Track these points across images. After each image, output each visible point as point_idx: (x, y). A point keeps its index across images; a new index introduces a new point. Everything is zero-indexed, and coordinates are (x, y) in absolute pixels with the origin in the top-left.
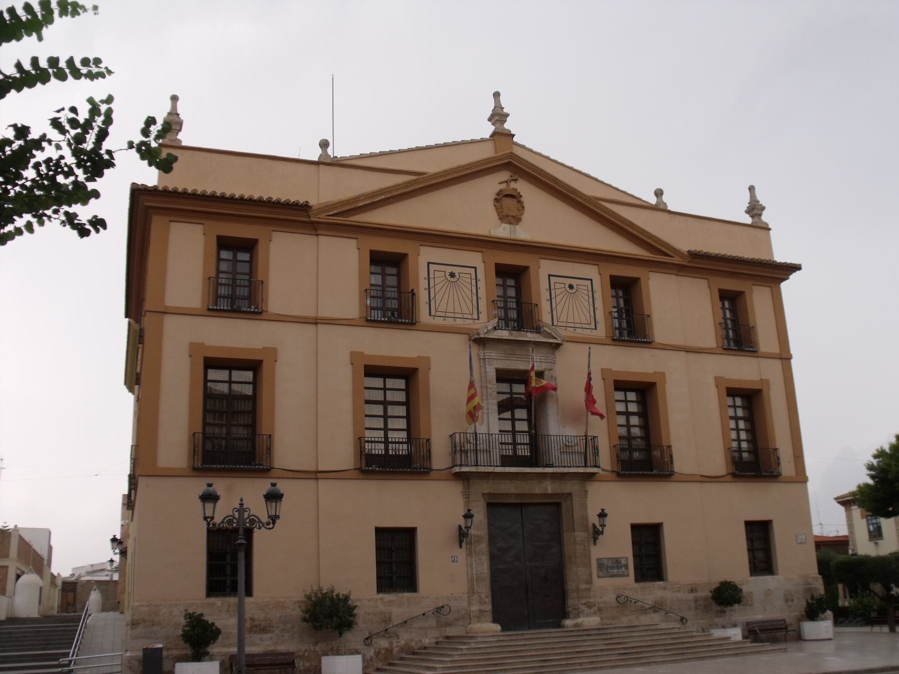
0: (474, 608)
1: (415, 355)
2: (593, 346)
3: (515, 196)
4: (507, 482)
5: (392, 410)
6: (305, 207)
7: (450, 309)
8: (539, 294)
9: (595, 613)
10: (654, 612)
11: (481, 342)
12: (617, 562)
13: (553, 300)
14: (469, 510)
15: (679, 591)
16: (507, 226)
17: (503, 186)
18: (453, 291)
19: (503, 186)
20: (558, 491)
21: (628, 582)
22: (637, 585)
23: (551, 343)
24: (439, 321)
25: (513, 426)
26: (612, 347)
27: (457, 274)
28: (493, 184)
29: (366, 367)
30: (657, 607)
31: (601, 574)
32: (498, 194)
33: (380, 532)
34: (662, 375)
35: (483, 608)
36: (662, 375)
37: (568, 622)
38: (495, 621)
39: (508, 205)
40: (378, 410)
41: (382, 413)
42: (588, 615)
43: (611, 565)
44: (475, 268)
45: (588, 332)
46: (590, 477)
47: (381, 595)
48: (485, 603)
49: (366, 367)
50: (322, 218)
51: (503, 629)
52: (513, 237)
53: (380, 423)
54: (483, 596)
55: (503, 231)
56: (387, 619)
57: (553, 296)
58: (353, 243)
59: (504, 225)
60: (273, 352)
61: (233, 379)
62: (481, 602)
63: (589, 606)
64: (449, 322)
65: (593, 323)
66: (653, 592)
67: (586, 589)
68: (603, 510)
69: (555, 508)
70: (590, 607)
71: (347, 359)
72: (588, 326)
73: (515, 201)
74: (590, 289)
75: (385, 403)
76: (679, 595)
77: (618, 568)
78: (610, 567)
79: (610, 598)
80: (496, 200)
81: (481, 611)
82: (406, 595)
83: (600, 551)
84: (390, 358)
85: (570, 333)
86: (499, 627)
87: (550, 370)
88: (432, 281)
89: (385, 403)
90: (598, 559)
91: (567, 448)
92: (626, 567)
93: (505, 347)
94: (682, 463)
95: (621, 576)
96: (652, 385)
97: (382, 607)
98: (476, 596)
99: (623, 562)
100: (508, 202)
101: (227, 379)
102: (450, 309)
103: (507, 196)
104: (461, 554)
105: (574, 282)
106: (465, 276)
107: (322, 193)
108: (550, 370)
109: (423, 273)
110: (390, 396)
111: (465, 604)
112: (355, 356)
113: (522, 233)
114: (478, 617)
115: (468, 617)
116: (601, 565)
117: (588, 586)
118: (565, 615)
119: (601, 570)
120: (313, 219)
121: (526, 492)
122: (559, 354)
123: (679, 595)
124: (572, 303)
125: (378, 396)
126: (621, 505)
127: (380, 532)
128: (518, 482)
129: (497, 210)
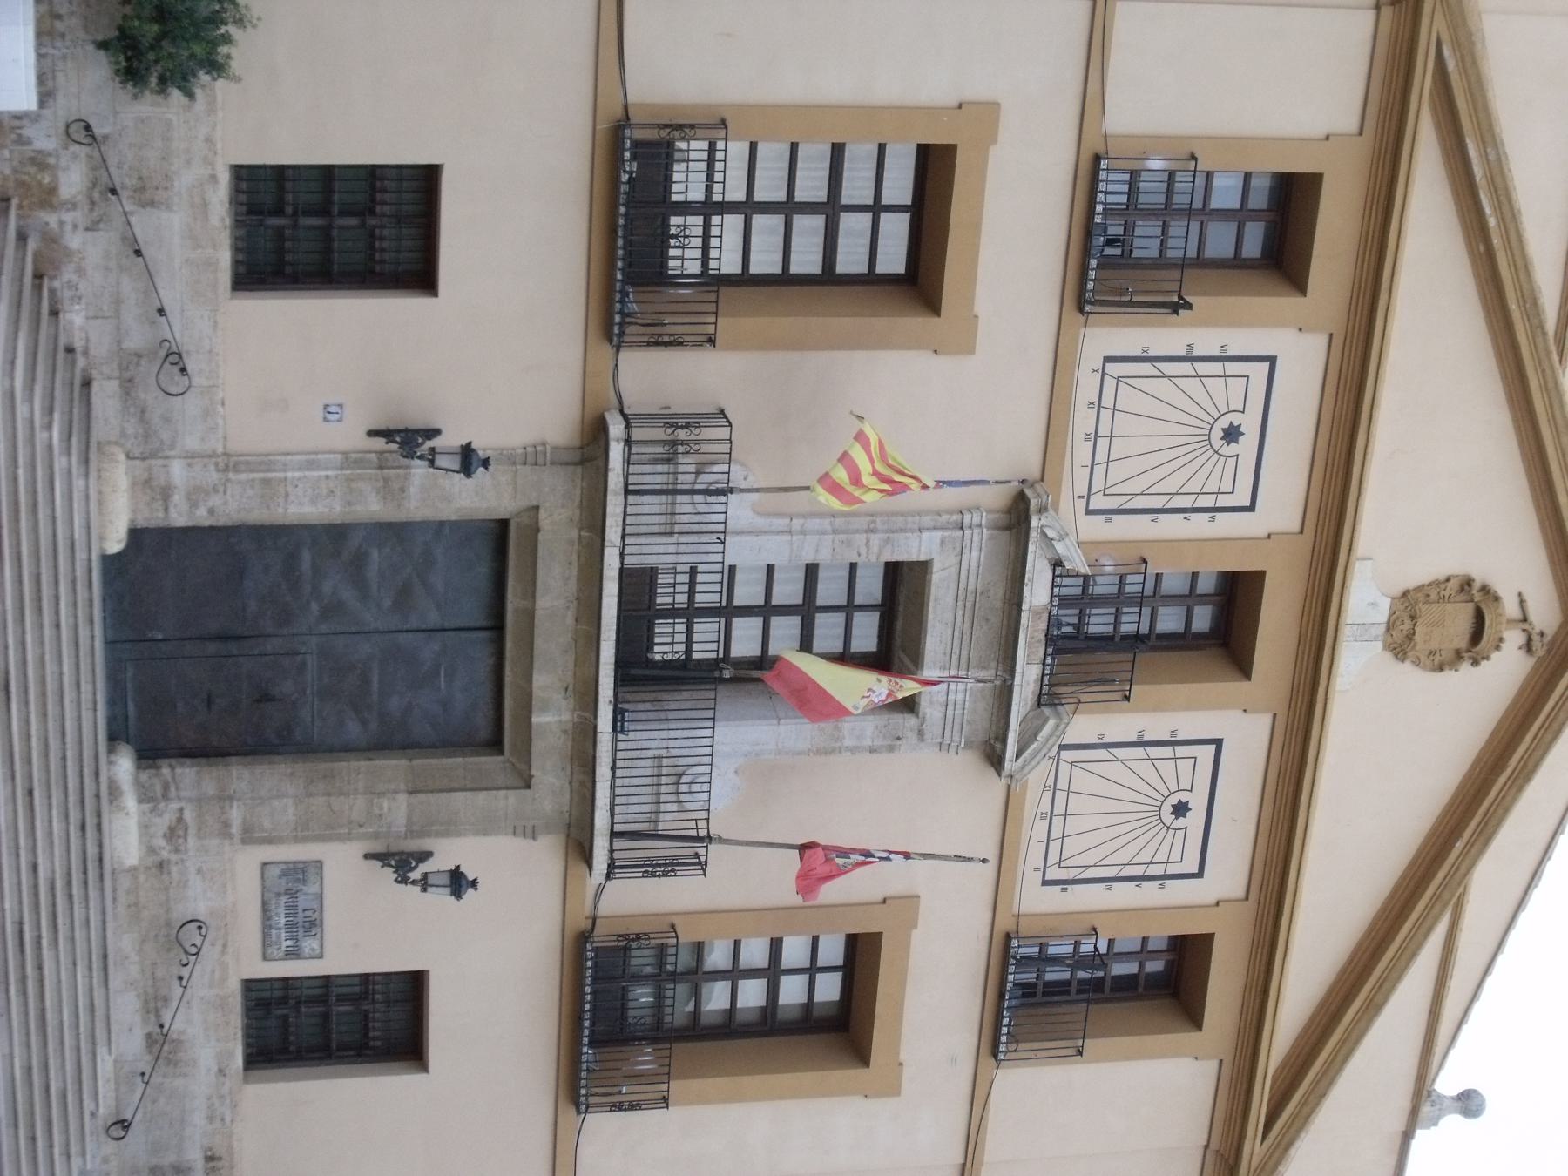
0: (178, 472)
1: (983, 304)
2: (989, 870)
4: (573, 585)
5: (809, 228)
7: (1124, 424)
8: (1158, 707)
9: (152, 850)
10: (149, 1036)
11: (1017, 517)
12: (307, 924)
14: (486, 463)
15: (211, 1119)
16: (1382, 615)
17: (1511, 608)
18: (1178, 438)
19: (1511, 608)
20: (538, 746)
22: (234, 986)
23: (1004, 741)
24: (1086, 387)
25: (747, 611)
26: (985, 932)
27: (1233, 449)
29: (949, 151)
30: (162, 1044)
31: (275, 871)
32: (1485, 589)
33: (425, 182)
34: (892, 1088)
36: (892, 1088)
37: (124, 765)
38: (135, 534)
40: (811, 187)
41: (800, 196)
42: (145, 828)
43: (302, 904)
44: (1251, 508)
45: (1035, 857)
46: (581, 850)
47: (225, 178)
48: (194, 505)
49: (949, 151)
51: (107, 560)
52: (1346, 632)
53: (770, 188)
54: (215, 500)
55: (1366, 599)
56: (148, 194)
58: (1350, 123)
59: (1385, 605)
62: (195, 495)
63: (175, 833)
64: (1083, 420)
66: (212, 1034)
67: (227, 825)
69: (488, 732)
71: (976, 90)
72: (1053, 858)
73: (1462, 642)
75: (831, 208)
76: (199, 1119)
77: (289, 927)
78: (293, 904)
79: (198, 900)
80: (1467, 583)
81: (166, 493)
82: (225, 257)
83: (344, 869)
84: (976, 227)
85: (1034, 798)
86: (115, 545)
87: (921, 734)
88: (1216, 368)
90: (319, 864)
91: (674, 778)
92: (294, 954)
93: (998, 593)
95: (265, 935)
96: (860, 1053)
97: (185, 179)
98: (214, 477)
99: (309, 945)
100: (1459, 621)
102: (1124, 424)
103: (1479, 618)
104: (350, 435)
105: (1195, 819)
106: (1226, 475)
108: (921, 734)
109: (1241, 341)
110: (854, 226)
111: (191, 442)
112: (985, 115)
113: (1358, 663)
114: (147, 482)
116: (299, 872)
117: (235, 829)
118: (148, 755)
119: (285, 874)
121: (539, 642)
122: (968, 764)
123: (199, 1119)
124: (1130, 810)
125: (856, 188)
127: (425, 182)
128: (570, 620)
129: (1436, 584)
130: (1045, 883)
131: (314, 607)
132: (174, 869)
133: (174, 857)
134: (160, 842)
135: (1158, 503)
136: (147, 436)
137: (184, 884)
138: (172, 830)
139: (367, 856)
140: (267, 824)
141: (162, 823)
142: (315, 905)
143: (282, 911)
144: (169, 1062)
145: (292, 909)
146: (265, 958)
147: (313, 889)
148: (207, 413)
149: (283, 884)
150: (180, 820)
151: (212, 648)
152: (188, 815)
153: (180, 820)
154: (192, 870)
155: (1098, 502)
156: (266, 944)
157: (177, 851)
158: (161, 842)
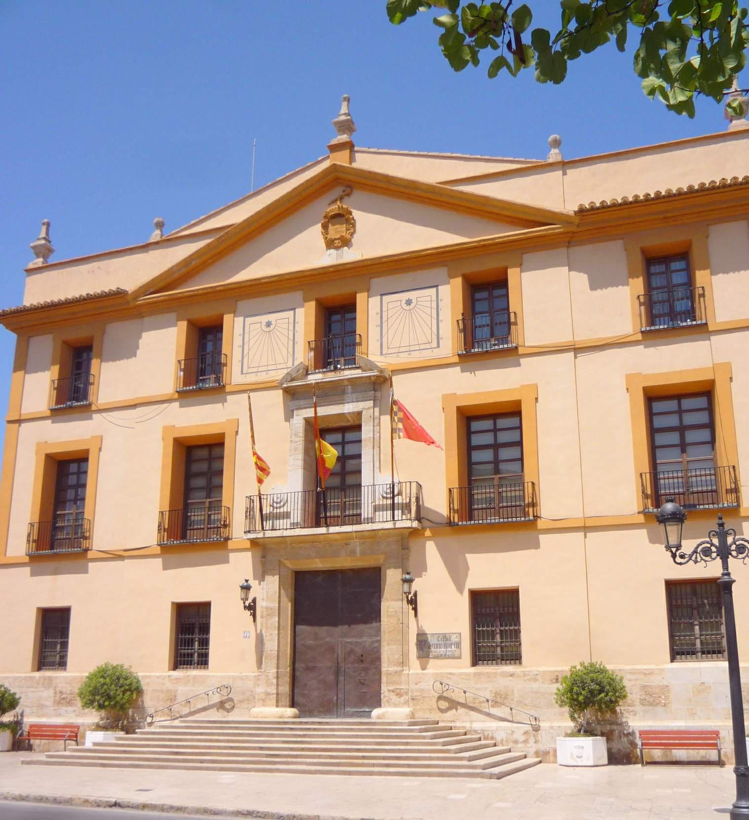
0: (260, 690)
2: (251, 394)
13: (385, 325)
15: (536, 680)
27: (273, 323)
30: (499, 700)
36: (446, 398)
37: (376, 712)
38: (293, 705)
42: (395, 705)
55: (329, 258)
56: (173, 698)
57: (385, 319)
61: (346, 440)
62: (269, 684)
64: (262, 377)
65: (435, 341)
67: (396, 672)
70: (399, 695)
72: (428, 346)
74: (434, 298)
76: (535, 686)
77: (446, 646)
81: (268, 694)
85: (404, 360)
86: (291, 711)
88: (246, 336)
92: (458, 645)
94: (549, 508)
97: (168, 685)
99: (454, 639)
101: (492, 427)
111: (251, 684)
112: (728, 366)
114: (263, 700)
115: (251, 700)
117: (399, 669)
118: (379, 704)
123: (535, 686)
130: (438, 346)
131: (328, 639)
132: (415, 694)
133: (410, 694)
135: (291, 343)
136: (248, 700)
137: (422, 690)
138: (397, 694)
140: (397, 656)
141: (394, 698)
142: (436, 637)
143: (438, 650)
144: (506, 698)
145: (438, 646)
146: (459, 658)
148: (242, 679)
150: (393, 691)
151: (341, 678)
152: (392, 688)
153: (393, 691)
154: (417, 687)
155: (435, 344)
156: (454, 658)
157: (407, 693)
158: (403, 698)
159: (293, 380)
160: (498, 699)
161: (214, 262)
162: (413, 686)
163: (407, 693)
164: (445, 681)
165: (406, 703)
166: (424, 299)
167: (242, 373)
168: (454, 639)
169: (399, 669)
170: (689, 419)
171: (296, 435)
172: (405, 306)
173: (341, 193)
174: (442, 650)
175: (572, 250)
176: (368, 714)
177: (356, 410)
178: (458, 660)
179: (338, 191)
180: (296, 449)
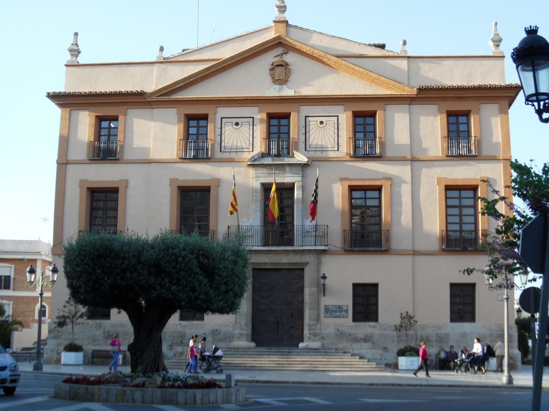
3: (284, 65)
4: (264, 255)
6: (141, 94)
12: (340, 308)
16: (277, 87)
17: (277, 59)
19: (275, 60)
21: (347, 322)
22: (354, 324)
28: (270, 58)
30: (367, 339)
31: (326, 315)
32: (272, 65)
35: (242, 332)
37: (301, 345)
39: (281, 73)
43: (335, 309)
46: (324, 252)
47: (181, 322)
48: (243, 329)
50: (154, 98)
51: (257, 346)
59: (275, 86)
60: (126, 183)
67: (314, 325)
68: (324, 274)
69: (298, 271)
71: (168, 183)
73: (283, 68)
77: (340, 312)
79: (331, 330)
80: (271, 70)
82: (196, 322)
83: (326, 301)
84: (193, 181)
89: (460, 207)
90: (325, 306)
91: (305, 233)
92: (347, 311)
99: (344, 308)
100: (279, 70)
103: (277, 66)
107: (151, 82)
113: (288, 92)
116: (327, 310)
117: (315, 323)
119: (327, 313)
120: (148, 100)
121: (276, 262)
126: (344, 272)
128: (270, 256)
129: (271, 76)
134: (317, 338)
135: (251, 137)
139: (324, 295)
140: (314, 316)
144: (371, 338)
145: (335, 312)
146: (347, 317)
147: (331, 307)
149: (329, 313)
153: (312, 334)
156: (344, 317)
159: (255, 160)
160: (367, 339)
161: (200, 82)
162: (323, 332)
163: (319, 335)
164: (340, 329)
165: (319, 340)
166: (330, 122)
167: (221, 151)
168: (344, 308)
169: (315, 323)
170: (465, 202)
171: (256, 192)
172: (319, 125)
173: (282, 52)
174: (338, 314)
175: (411, 106)
176: (297, 346)
177: (292, 181)
178: (346, 319)
179: (279, 51)
180: (256, 200)
